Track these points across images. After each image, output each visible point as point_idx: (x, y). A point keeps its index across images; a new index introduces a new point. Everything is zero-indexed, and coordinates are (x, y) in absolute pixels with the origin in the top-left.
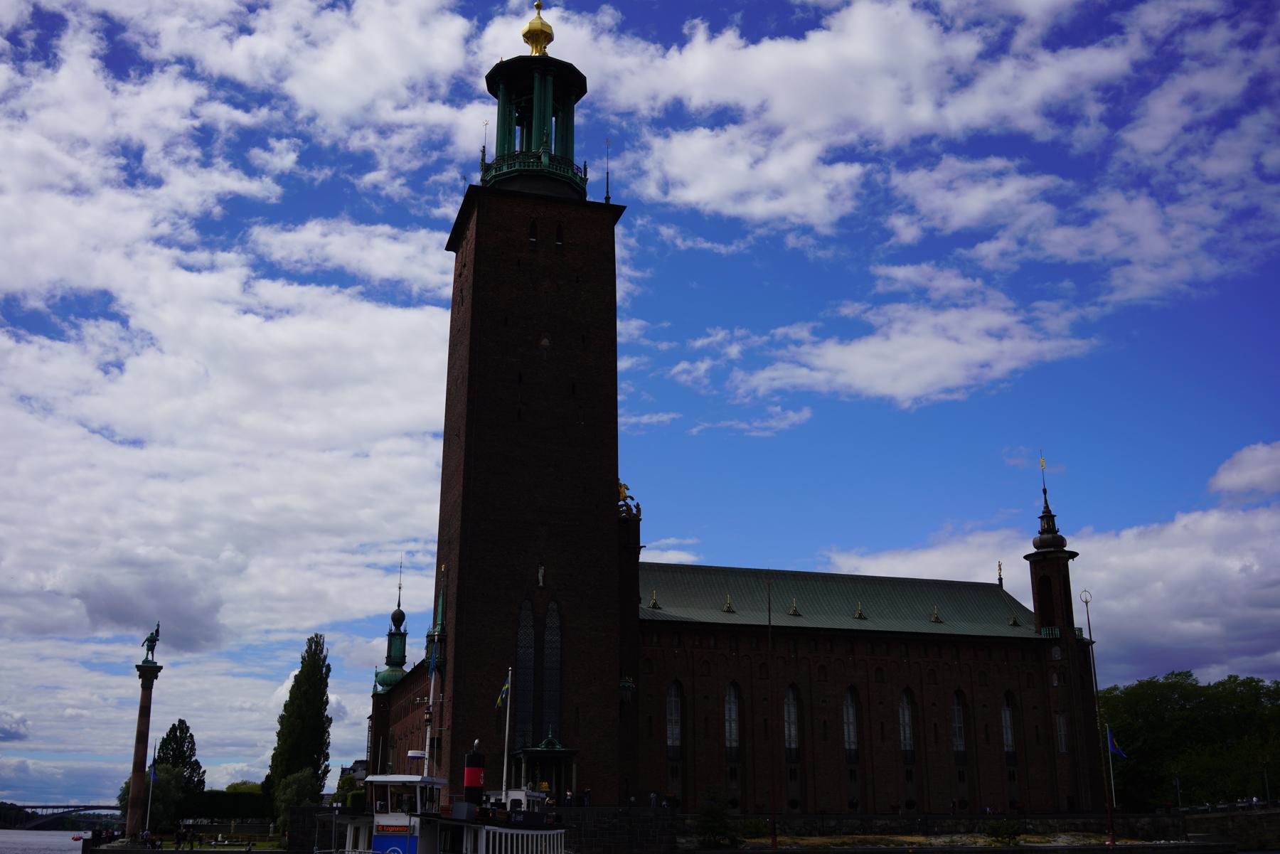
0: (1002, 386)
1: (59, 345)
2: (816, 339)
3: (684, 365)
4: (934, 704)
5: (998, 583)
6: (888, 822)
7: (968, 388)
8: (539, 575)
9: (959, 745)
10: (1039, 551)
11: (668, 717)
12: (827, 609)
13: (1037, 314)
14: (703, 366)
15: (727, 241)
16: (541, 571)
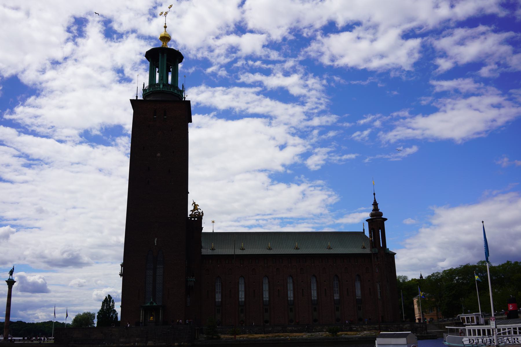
0: (502, 129)
1: (110, 148)
2: (412, 116)
3: (358, 133)
4: (325, 281)
5: (363, 231)
6: (293, 328)
7: (487, 131)
8: (155, 241)
9: (336, 297)
10: (372, 218)
11: (216, 291)
12: (284, 246)
13: (513, 96)
14: (366, 133)
15: (365, 79)
16: (156, 240)
